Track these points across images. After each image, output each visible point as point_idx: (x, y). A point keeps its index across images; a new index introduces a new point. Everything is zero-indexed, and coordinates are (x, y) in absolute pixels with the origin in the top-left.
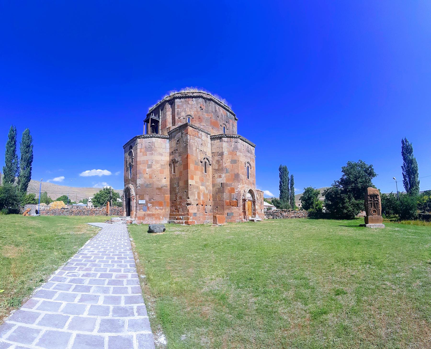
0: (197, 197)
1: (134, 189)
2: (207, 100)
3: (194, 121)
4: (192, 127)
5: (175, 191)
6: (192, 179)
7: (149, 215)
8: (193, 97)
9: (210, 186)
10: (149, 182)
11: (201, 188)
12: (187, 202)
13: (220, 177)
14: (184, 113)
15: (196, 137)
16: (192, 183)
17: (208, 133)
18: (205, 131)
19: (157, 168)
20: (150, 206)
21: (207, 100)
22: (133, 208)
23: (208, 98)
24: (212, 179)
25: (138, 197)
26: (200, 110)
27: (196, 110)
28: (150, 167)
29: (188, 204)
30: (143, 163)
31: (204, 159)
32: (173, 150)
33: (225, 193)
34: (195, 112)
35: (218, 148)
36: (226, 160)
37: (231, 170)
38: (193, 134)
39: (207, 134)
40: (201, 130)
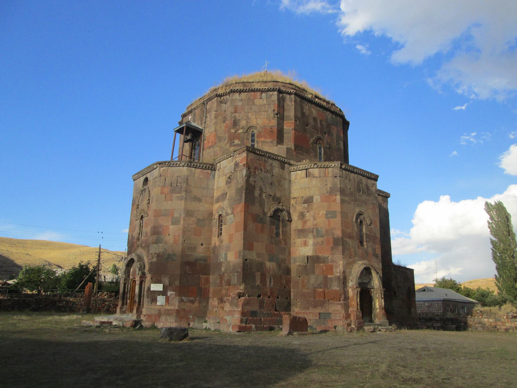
0: (259, 282)
4: (255, 153)
8: (262, 91)
10: (172, 251)
13: (305, 244)
15: (261, 170)
16: (249, 257)
20: (171, 294)
23: (288, 91)
26: (274, 115)
30: (164, 215)
37: (327, 231)
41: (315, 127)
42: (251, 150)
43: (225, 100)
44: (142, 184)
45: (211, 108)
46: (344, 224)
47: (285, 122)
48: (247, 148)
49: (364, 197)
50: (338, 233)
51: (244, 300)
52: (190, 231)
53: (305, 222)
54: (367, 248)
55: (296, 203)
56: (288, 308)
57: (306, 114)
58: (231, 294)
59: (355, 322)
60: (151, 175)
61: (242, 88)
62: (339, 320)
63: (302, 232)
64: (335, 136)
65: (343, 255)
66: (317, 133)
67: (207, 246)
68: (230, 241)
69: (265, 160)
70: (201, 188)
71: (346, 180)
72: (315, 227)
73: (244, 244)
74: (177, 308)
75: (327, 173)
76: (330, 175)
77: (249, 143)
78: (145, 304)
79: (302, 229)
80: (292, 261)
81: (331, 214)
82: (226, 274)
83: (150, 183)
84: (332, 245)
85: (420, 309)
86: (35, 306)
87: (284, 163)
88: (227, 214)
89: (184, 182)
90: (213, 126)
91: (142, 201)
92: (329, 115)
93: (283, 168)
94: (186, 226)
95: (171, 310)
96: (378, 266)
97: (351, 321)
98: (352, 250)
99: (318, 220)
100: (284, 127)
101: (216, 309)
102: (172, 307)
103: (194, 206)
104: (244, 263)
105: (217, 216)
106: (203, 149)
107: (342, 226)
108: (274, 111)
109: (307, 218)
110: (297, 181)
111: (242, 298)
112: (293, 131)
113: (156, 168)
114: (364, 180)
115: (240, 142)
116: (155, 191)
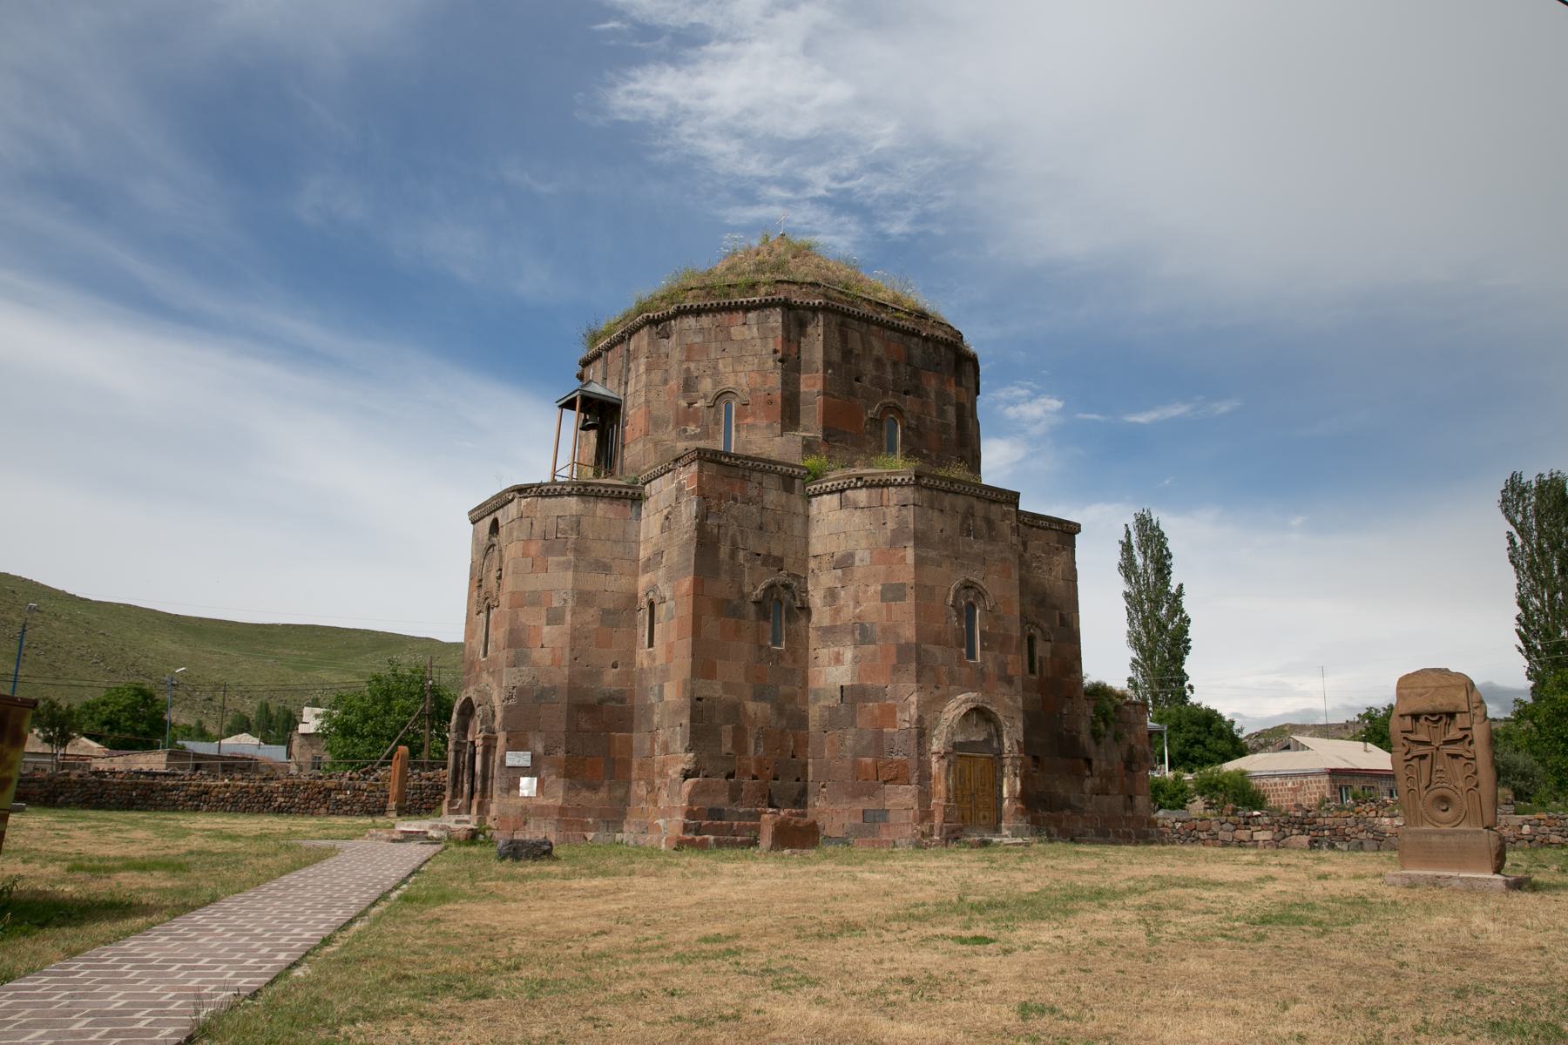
0: (729, 745)
3: (747, 417)
5: (650, 721)
11: (751, 707)
13: (838, 660)
14: (709, 380)
15: (735, 499)
18: (779, 468)
19: (588, 623)
26: (775, 364)
30: (532, 604)
34: (753, 374)
36: (862, 587)
38: (721, 490)
42: (705, 457)
44: (487, 531)
45: (637, 350)
46: (922, 612)
47: (803, 377)
48: (699, 453)
49: (978, 547)
50: (908, 633)
51: (695, 785)
53: (837, 612)
54: (984, 661)
55: (819, 568)
56: (800, 800)
58: (670, 772)
59: (941, 830)
60: (503, 515)
62: (904, 824)
63: (829, 632)
64: (932, 395)
65: (918, 682)
66: (885, 393)
68: (669, 661)
69: (744, 476)
73: (693, 664)
74: (560, 802)
75: (885, 497)
76: (892, 503)
78: (495, 796)
80: (811, 697)
81: (892, 593)
82: (661, 731)
83: (503, 531)
84: (895, 661)
85: (1274, 796)
86: (282, 800)
87: (790, 476)
88: (663, 600)
89: (572, 529)
90: (643, 393)
91: (488, 571)
95: (547, 807)
97: (932, 827)
100: (799, 388)
101: (643, 805)
102: (551, 801)
103: (595, 581)
104: (693, 708)
105: (644, 603)
106: (623, 446)
107: (917, 616)
108: (775, 351)
109: (842, 602)
110: (821, 517)
111: (690, 781)
112: (821, 397)
113: (513, 500)
114: (979, 507)
116: (512, 550)
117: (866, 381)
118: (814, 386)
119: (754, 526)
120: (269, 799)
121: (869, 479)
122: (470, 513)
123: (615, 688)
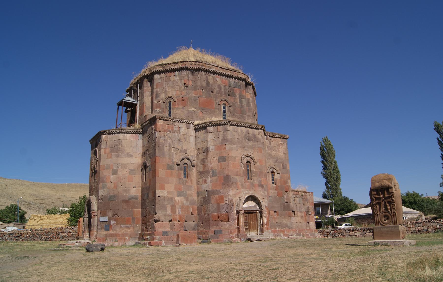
1: (96, 202)
2: (194, 71)
3: (176, 105)
4: (164, 120)
6: (163, 188)
7: (112, 236)
9: (193, 196)
11: (177, 198)
12: (155, 219)
14: (164, 94)
17: (190, 123)
18: (185, 121)
19: (125, 174)
21: (194, 71)
22: (93, 228)
23: (195, 68)
24: (196, 186)
25: (99, 213)
27: (179, 89)
28: (115, 173)
29: (156, 221)
30: (107, 169)
31: (183, 159)
32: (145, 150)
33: (210, 205)
34: (178, 92)
35: (203, 142)
36: (212, 158)
38: (165, 129)
39: (188, 123)
40: (177, 121)
41: (220, 93)
43: (151, 79)
49: (251, 143)
52: (125, 179)
57: (211, 83)
58: (151, 221)
61: (161, 69)
64: (238, 96)
66: (221, 96)
67: (138, 188)
68: (150, 185)
70: (131, 147)
71: (234, 133)
72: (211, 169)
75: (219, 128)
76: (221, 130)
77: (167, 110)
79: (203, 171)
84: (223, 181)
86: (45, 237)
92: (232, 81)
93: (189, 128)
94: (122, 175)
96: (263, 194)
98: (240, 183)
99: (213, 164)
115: (161, 110)
117: (215, 91)
118: (197, 94)
119: (176, 140)
120: (41, 237)
121: (213, 123)
122: (90, 141)
123: (134, 195)
